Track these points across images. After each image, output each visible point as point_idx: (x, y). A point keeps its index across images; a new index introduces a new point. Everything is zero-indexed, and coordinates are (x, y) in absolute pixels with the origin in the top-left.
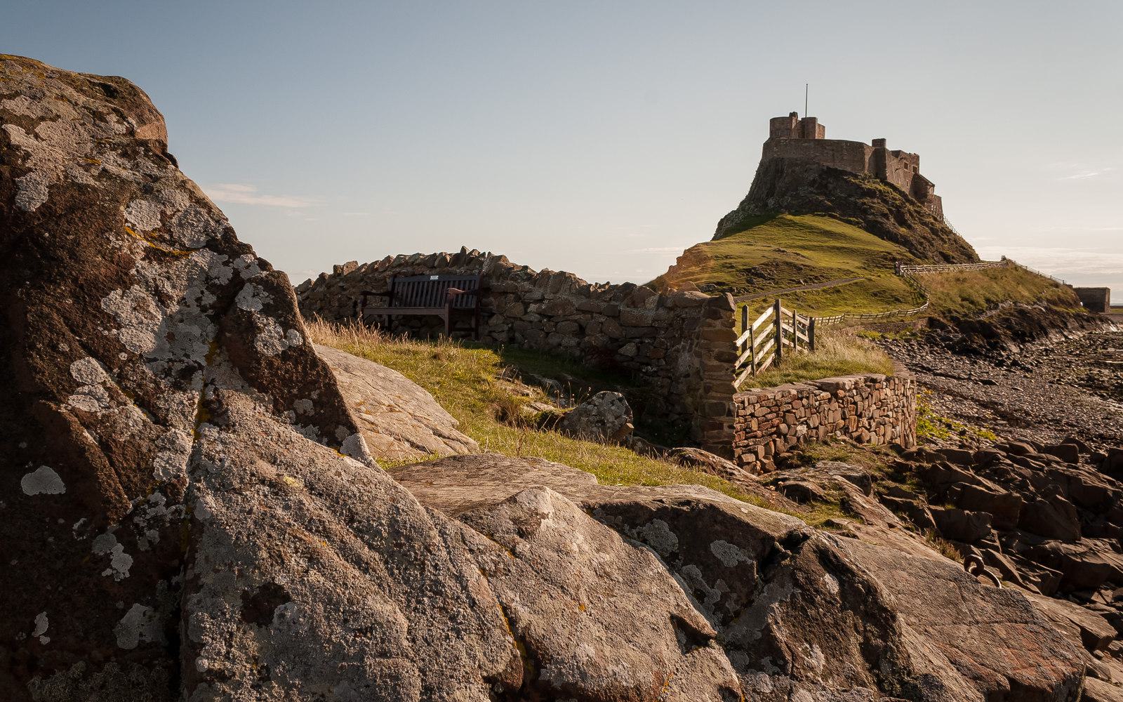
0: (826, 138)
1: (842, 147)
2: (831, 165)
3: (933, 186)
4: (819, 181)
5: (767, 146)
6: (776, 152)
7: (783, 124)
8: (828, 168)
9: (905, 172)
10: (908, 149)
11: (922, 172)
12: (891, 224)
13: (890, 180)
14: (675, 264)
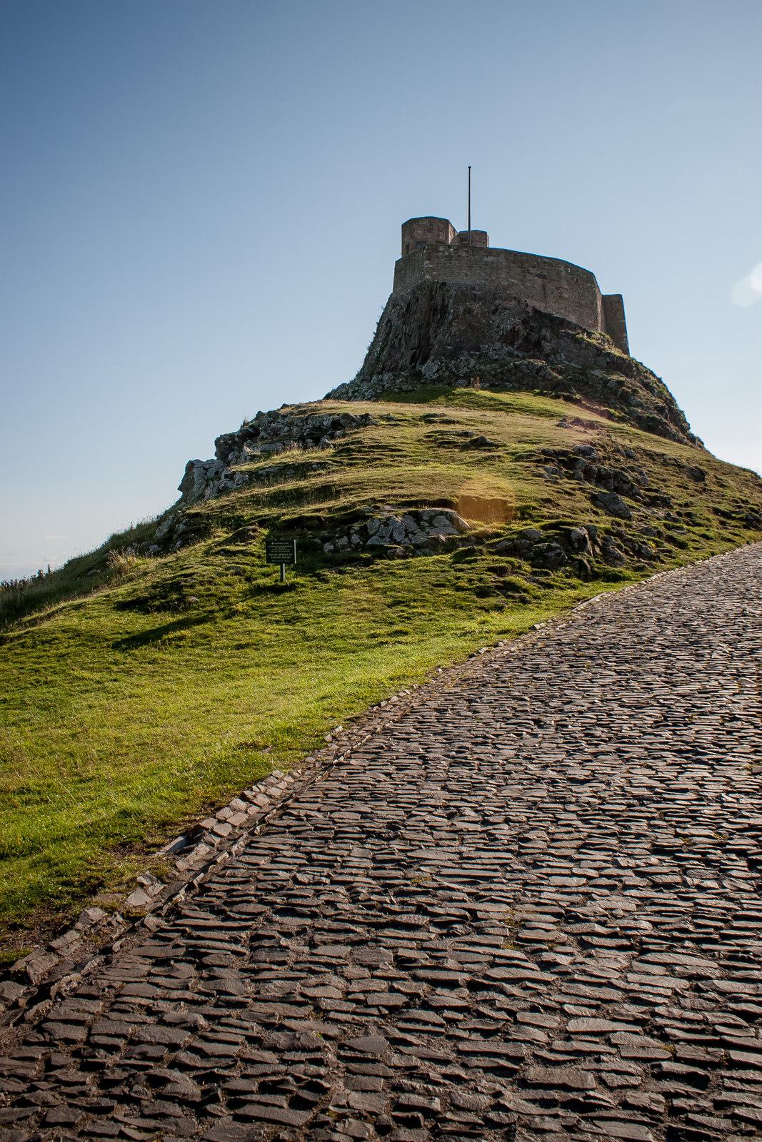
1: (558, 273)
2: (541, 306)
4: (523, 332)
5: (401, 268)
6: (429, 271)
7: (430, 230)
8: (536, 311)
14: (208, 453)
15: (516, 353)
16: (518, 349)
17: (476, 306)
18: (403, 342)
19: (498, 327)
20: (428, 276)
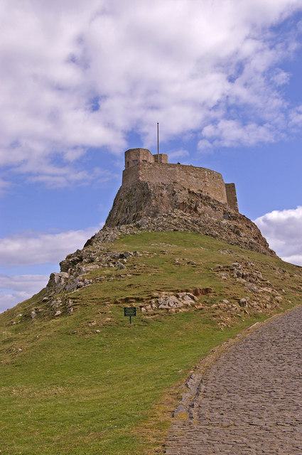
5: (125, 174)
17: (164, 192)
18: (128, 210)
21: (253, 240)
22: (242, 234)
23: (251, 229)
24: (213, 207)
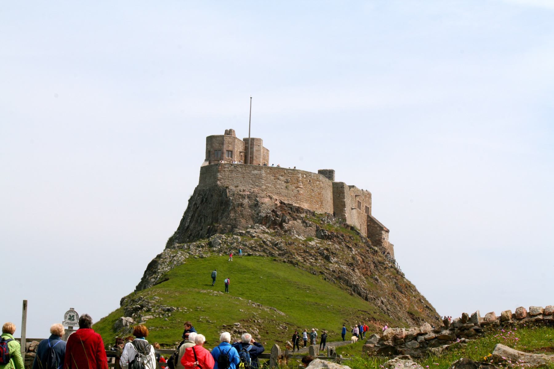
0: (273, 162)
3: (388, 231)
5: (204, 171)
8: (281, 203)
9: (359, 213)
10: (360, 186)
11: (375, 214)
12: (357, 277)
13: (349, 222)
15: (267, 230)
16: (268, 228)
17: (246, 201)
19: (258, 214)
20: (218, 183)
21: (345, 267)
22: (333, 260)
23: (351, 251)
24: (304, 222)
